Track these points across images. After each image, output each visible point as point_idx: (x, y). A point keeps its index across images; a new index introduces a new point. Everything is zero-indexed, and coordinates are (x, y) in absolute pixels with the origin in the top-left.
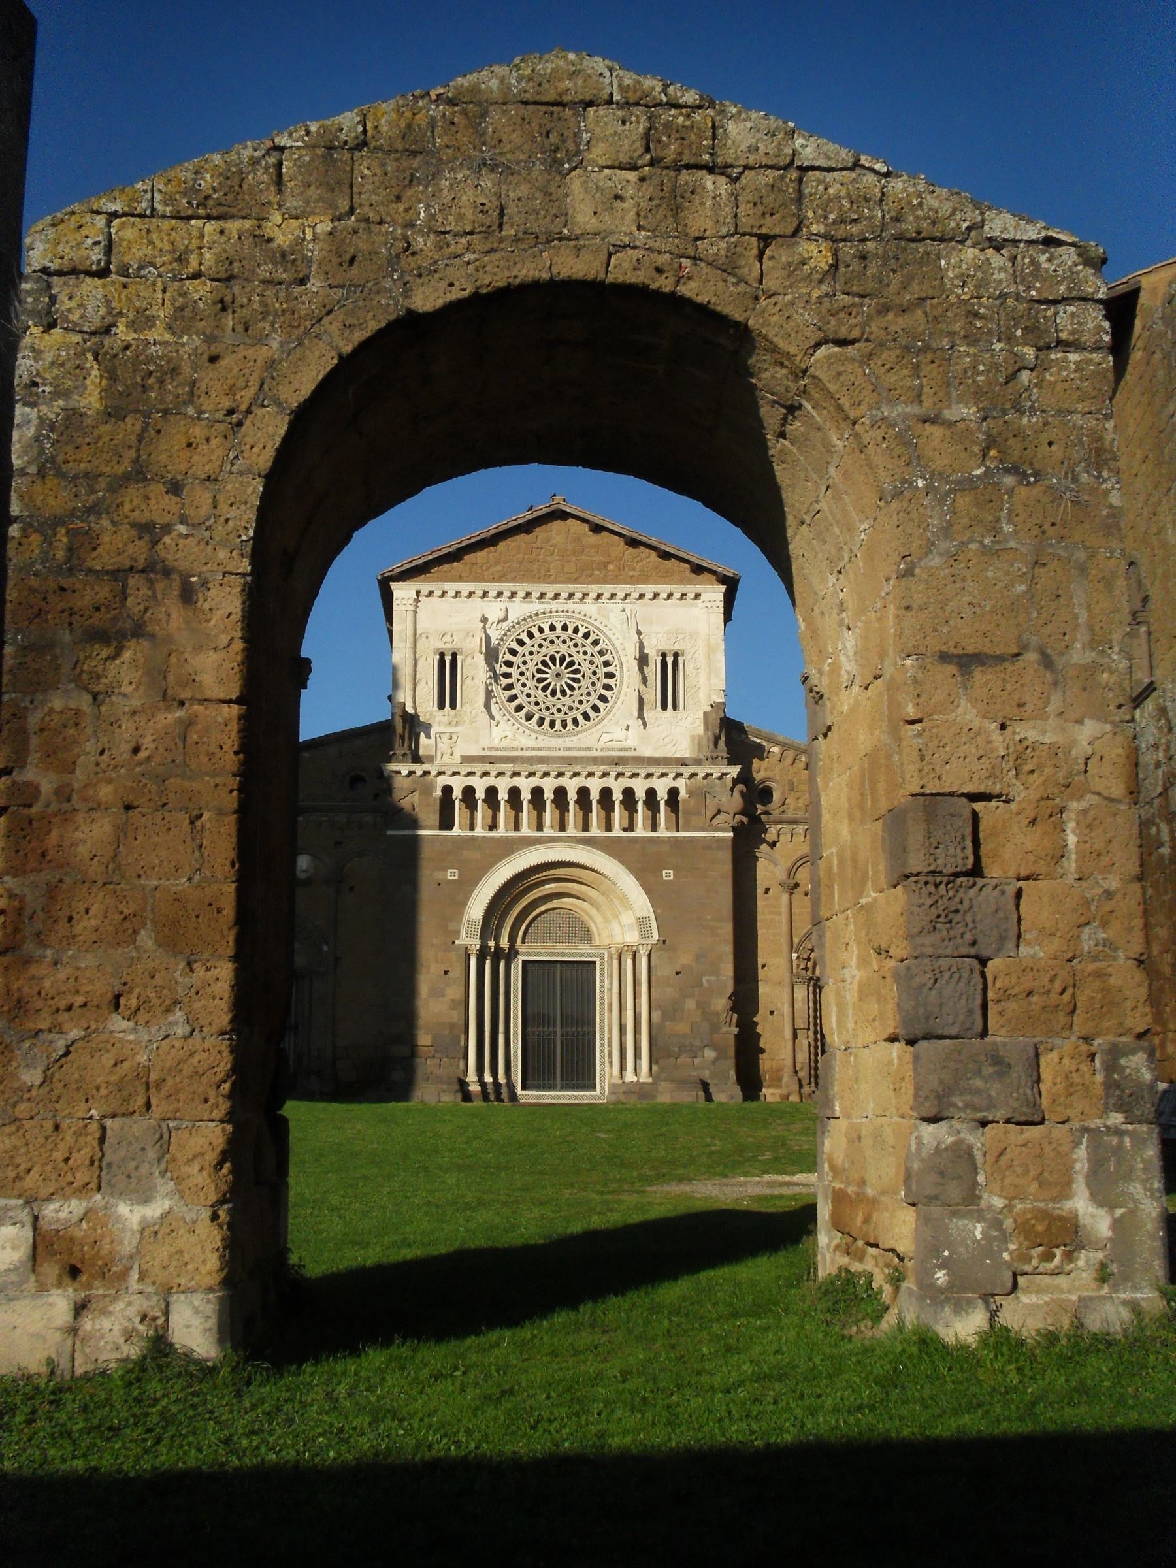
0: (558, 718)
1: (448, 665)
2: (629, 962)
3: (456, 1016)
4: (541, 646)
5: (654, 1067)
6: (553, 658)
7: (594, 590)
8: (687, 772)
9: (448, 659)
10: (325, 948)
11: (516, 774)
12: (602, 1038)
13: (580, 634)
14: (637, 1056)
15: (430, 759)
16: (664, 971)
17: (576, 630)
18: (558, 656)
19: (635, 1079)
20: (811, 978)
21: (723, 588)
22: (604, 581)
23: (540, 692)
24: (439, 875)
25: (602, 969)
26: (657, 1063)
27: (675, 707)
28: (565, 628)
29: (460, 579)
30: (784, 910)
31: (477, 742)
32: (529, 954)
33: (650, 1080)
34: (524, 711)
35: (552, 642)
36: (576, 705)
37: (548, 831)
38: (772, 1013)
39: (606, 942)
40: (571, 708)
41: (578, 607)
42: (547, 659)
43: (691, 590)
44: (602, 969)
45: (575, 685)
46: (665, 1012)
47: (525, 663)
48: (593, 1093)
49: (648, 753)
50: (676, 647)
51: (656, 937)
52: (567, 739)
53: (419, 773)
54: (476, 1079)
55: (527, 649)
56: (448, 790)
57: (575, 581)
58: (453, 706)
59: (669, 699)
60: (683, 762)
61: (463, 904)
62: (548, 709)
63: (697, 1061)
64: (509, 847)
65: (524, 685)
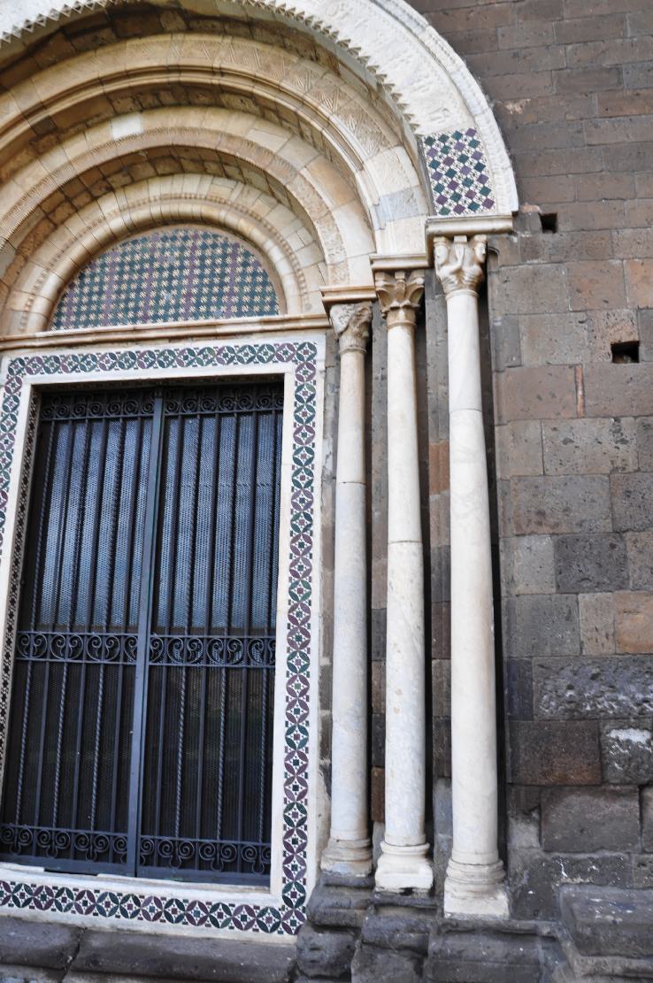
2: (397, 342)
12: (298, 670)
14: (436, 768)
19: (421, 877)
25: (305, 400)
33: (497, 907)
44: (305, 400)
51: (506, 198)
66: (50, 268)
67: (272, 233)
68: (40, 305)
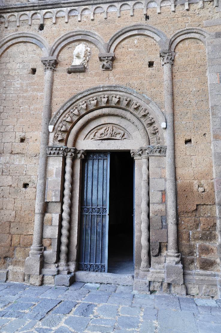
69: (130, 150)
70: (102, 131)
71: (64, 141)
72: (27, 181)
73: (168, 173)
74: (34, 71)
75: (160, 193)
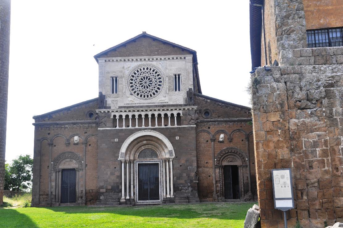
0: (146, 94)
1: (115, 80)
2: (167, 163)
3: (118, 180)
4: (141, 74)
5: (175, 193)
6: (144, 78)
7: (155, 57)
8: (182, 108)
9: (114, 79)
10: (83, 162)
11: (134, 111)
12: (161, 185)
13: (152, 70)
15: (110, 108)
16: (178, 166)
17: (150, 69)
18: (145, 77)
19: (170, 196)
20: (220, 166)
21: (192, 55)
22: (158, 55)
23: (141, 87)
24: (112, 140)
26: (175, 192)
27: (179, 90)
28: (147, 69)
29: (117, 56)
30: (212, 147)
31: (123, 102)
32: (140, 162)
33: (173, 197)
34: (137, 93)
35: (144, 73)
36: (151, 91)
37: (143, 127)
38: (209, 176)
39: (161, 157)
40: (149, 92)
41: (151, 63)
42: (143, 78)
43: (183, 56)
45: (151, 85)
46: (177, 177)
47: (136, 79)
48: (159, 201)
49: (171, 103)
50: (179, 73)
51: (174, 156)
52: (148, 101)
53: (106, 112)
54: (124, 198)
55: (137, 75)
56: (115, 116)
57: (150, 55)
58: (116, 92)
59: (177, 87)
60: (181, 105)
61: (119, 148)
62: (143, 92)
63: (187, 191)
64: (132, 132)
65: (136, 86)
66: (138, 153)
67: (157, 151)
68: (137, 156)
69: (237, 165)
70: (228, 159)
71: (219, 163)
72: (210, 175)
73: (248, 172)
74: (207, 141)
75: (246, 178)
